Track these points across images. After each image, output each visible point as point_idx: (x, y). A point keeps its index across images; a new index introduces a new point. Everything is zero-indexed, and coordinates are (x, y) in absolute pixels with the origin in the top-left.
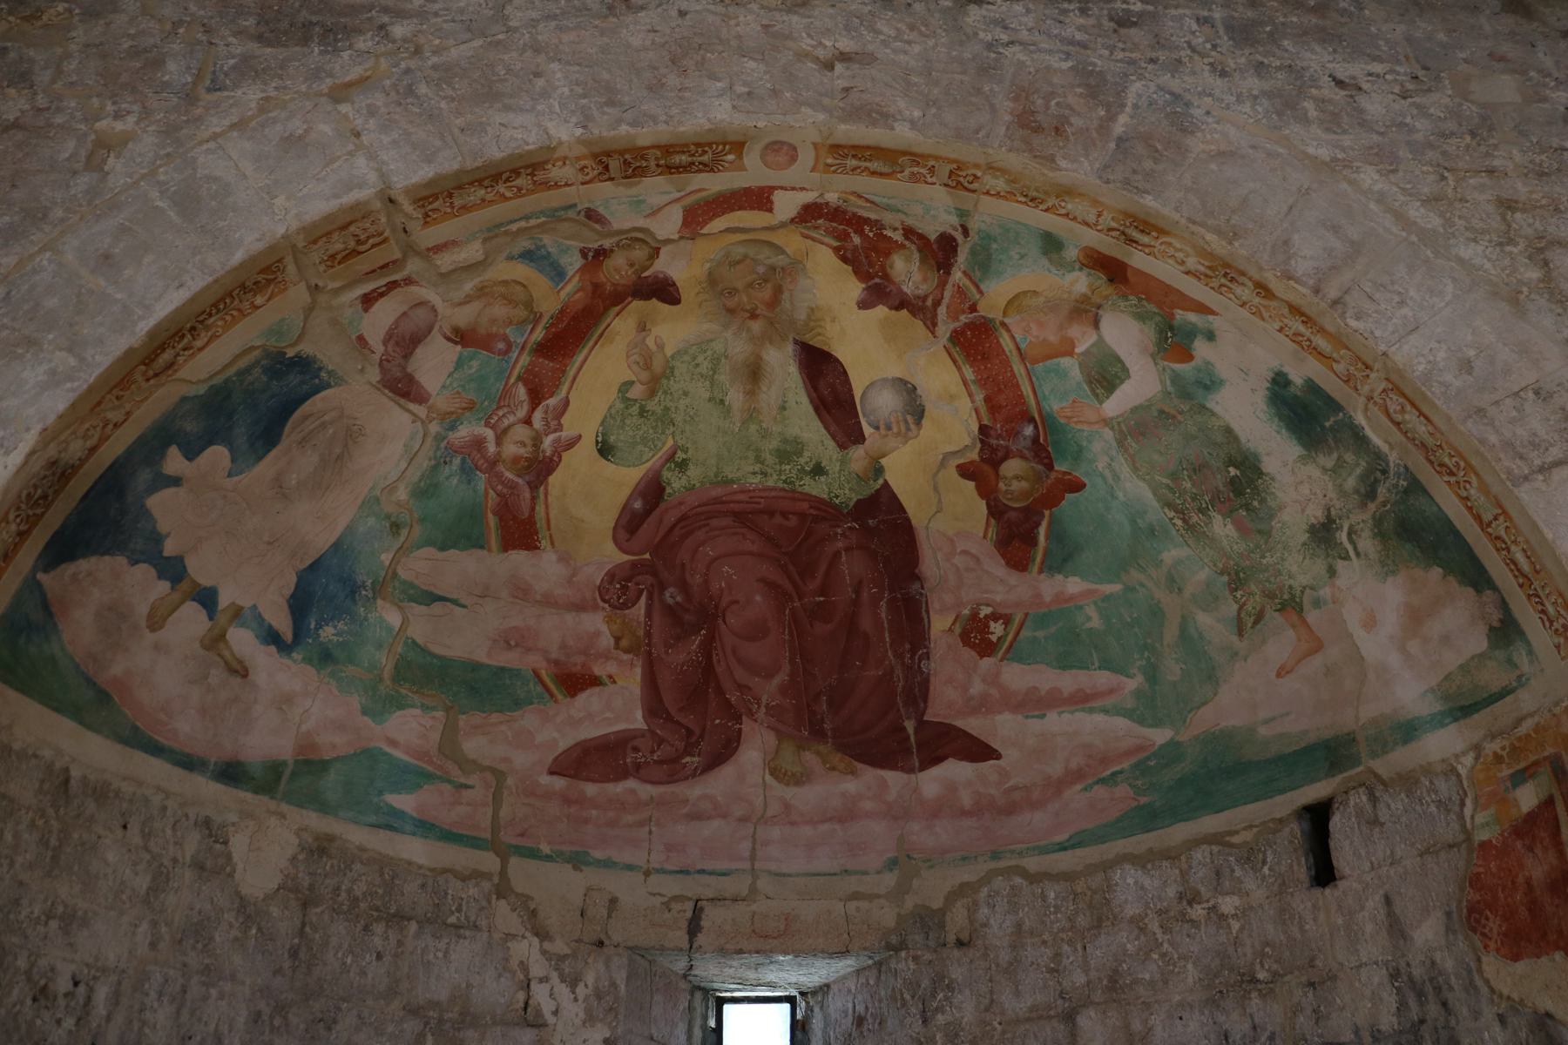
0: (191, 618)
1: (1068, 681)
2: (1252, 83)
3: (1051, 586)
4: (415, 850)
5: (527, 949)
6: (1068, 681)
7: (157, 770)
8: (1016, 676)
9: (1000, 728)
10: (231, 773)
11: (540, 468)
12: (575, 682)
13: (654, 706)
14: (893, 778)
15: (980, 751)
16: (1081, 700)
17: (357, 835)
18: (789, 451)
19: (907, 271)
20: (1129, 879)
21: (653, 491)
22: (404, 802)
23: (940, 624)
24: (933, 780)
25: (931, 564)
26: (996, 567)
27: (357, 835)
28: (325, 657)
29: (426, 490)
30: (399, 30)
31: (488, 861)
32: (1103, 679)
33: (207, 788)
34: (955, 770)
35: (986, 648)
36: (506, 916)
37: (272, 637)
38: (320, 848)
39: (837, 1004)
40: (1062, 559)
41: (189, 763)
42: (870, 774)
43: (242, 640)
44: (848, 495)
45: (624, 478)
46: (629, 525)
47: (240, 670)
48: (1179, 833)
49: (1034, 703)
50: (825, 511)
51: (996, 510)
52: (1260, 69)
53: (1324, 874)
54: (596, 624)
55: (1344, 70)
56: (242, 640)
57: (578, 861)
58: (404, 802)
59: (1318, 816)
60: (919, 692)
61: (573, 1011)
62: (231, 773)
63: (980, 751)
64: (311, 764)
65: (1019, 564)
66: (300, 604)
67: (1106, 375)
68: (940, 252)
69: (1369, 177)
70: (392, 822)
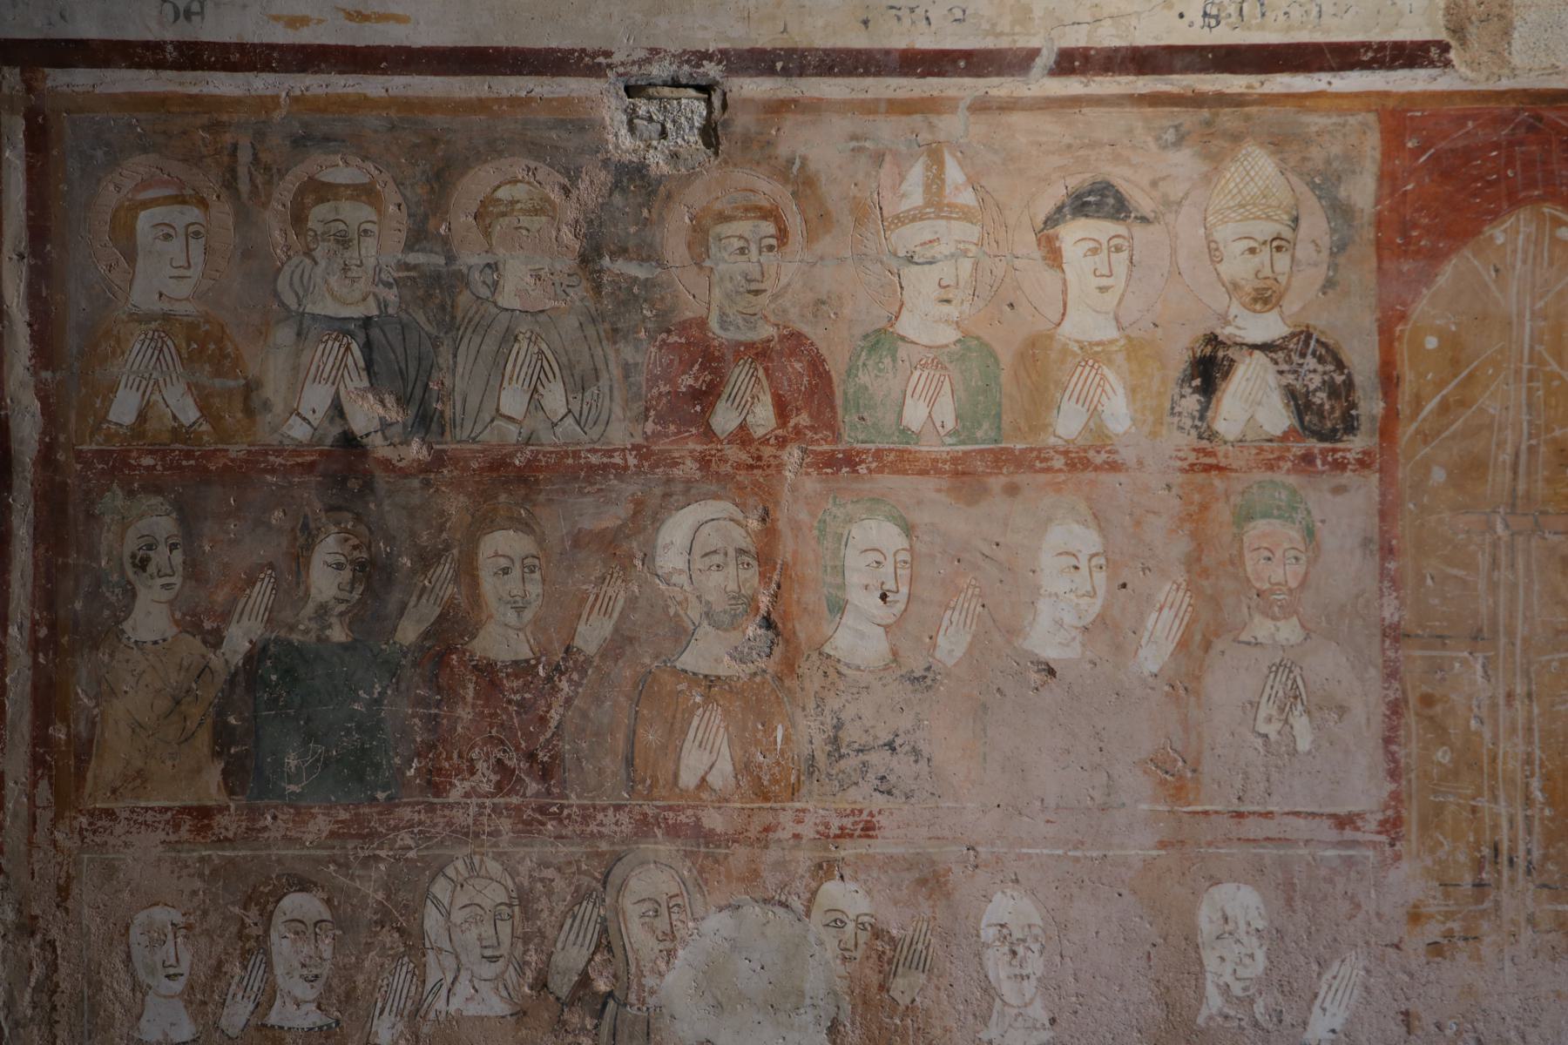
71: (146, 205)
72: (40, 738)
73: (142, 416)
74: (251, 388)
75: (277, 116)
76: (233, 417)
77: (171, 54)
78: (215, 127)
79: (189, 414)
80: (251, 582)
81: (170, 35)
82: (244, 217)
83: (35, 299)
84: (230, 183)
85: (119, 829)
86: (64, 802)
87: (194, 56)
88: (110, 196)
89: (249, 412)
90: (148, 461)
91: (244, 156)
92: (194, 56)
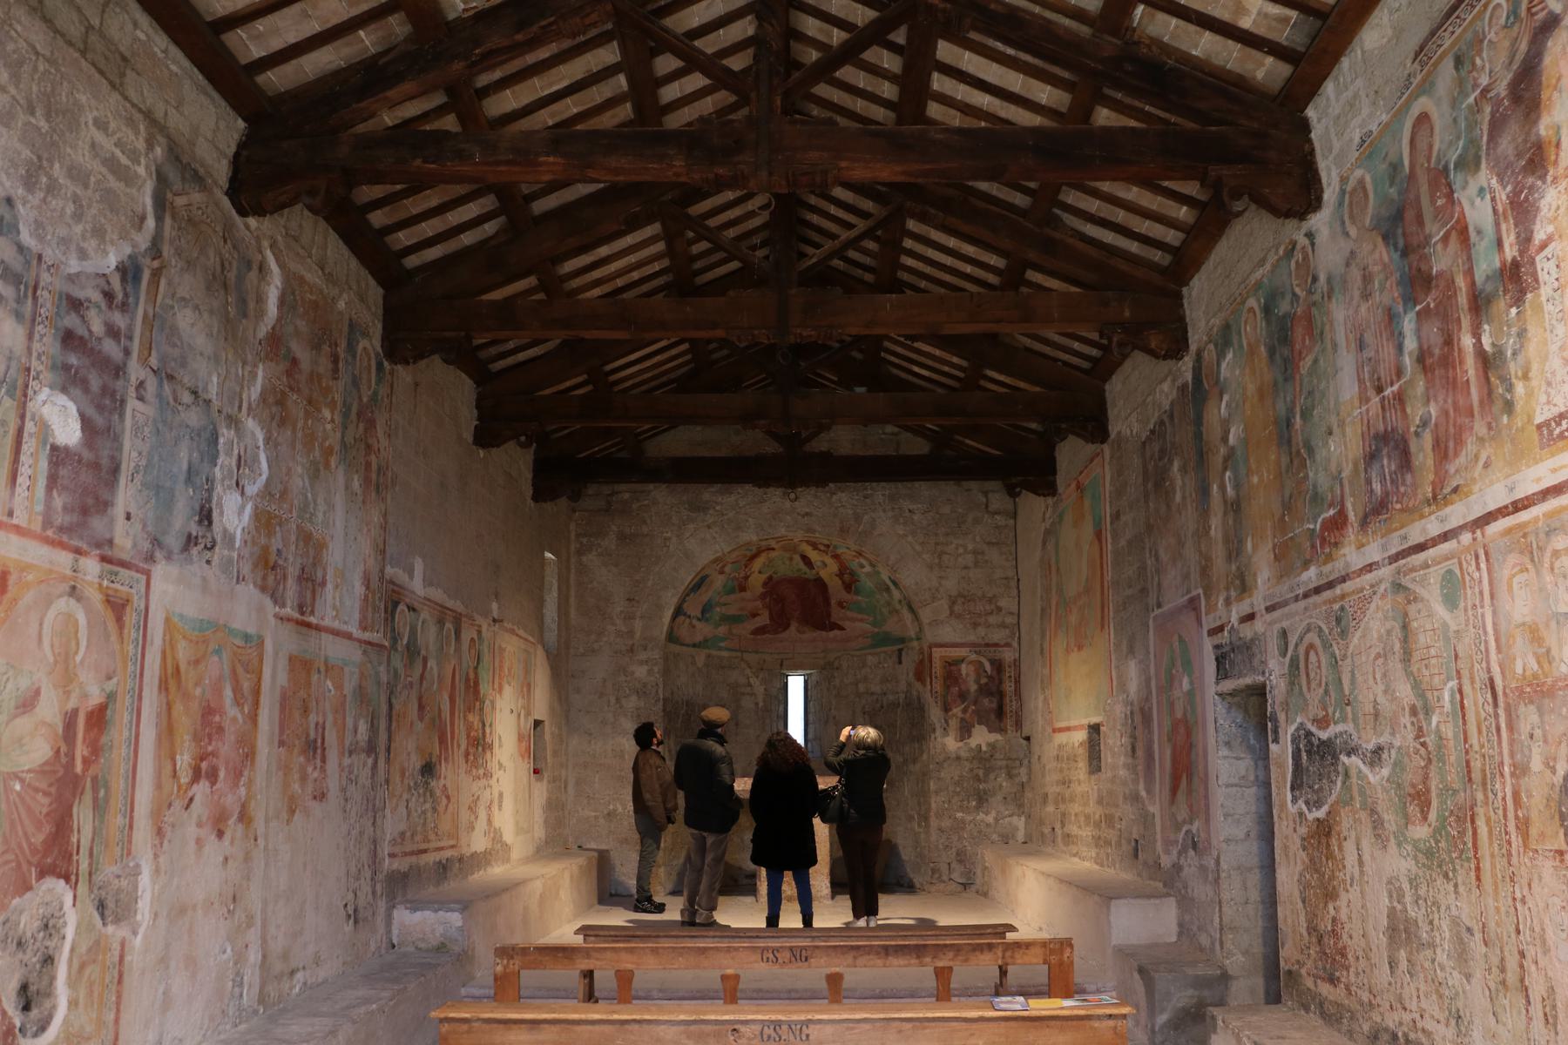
0: (688, 621)
1: (860, 616)
2: (890, 514)
3: (855, 597)
4: (725, 654)
5: (748, 671)
6: (860, 616)
7: (684, 648)
8: (849, 614)
9: (846, 624)
10: (694, 646)
11: (746, 578)
12: (754, 615)
13: (771, 618)
14: (824, 633)
15: (841, 628)
16: (862, 620)
17: (714, 653)
18: (799, 570)
19: (822, 548)
20: (870, 657)
21: (770, 578)
22: (722, 644)
23: (833, 602)
24: (832, 634)
25: (831, 590)
26: (844, 592)
27: (714, 653)
28: (707, 620)
29: (724, 586)
30: (718, 508)
31: (739, 654)
32: (865, 617)
33: (692, 649)
34: (836, 632)
35: (843, 608)
36: (743, 665)
37: (699, 620)
38: (709, 656)
39: (814, 678)
40: (857, 593)
41: (688, 645)
42: (819, 632)
43: (695, 622)
44: (812, 577)
45: (764, 577)
46: (765, 584)
47: (694, 627)
48: (879, 650)
49: (853, 620)
50: (807, 580)
51: (843, 582)
52: (893, 509)
53: (900, 663)
54: (759, 604)
55: (911, 507)
56: (695, 622)
57: (757, 652)
58: (722, 644)
59: (900, 651)
60: (829, 615)
61: (758, 683)
62: (694, 646)
63: (841, 628)
64: (706, 641)
65: (849, 592)
66: (703, 612)
67: (862, 566)
68: (828, 546)
69: (910, 538)
70: (720, 649)
71: (1514, 576)
72: (1517, 817)
73: (1524, 670)
74: (1548, 651)
75: (1540, 524)
76: (1546, 666)
77: (1511, 508)
78: (1525, 536)
79: (1536, 667)
80: (1560, 743)
81: (1508, 501)
82: (1538, 573)
83: (1494, 624)
84: (1532, 560)
85: (1541, 858)
86: (1526, 846)
87: (1518, 506)
88: (1506, 573)
89: (1550, 663)
90: (1528, 690)
91: (1535, 546)
92: (1518, 506)
